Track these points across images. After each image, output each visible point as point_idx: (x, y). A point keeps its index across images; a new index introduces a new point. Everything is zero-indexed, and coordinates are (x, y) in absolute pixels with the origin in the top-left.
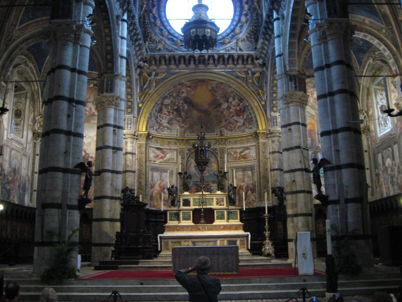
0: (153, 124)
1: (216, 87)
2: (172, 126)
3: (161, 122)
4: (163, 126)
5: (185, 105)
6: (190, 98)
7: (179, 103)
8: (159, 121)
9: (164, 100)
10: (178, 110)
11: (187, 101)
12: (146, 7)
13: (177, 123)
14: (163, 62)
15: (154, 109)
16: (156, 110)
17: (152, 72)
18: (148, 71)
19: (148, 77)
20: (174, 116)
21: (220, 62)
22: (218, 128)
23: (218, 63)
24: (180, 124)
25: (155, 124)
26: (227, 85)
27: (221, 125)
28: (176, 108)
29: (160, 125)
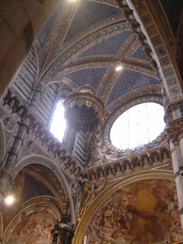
0: (93, 238)
1: (157, 187)
2: (117, 240)
3: (104, 236)
4: (106, 240)
5: (130, 214)
6: (134, 205)
7: (122, 213)
8: (101, 235)
9: (105, 211)
10: (122, 221)
11: (130, 209)
12: (92, 136)
13: (122, 235)
14: (101, 175)
15: (94, 222)
16: (97, 224)
17: (91, 186)
18: (89, 186)
19: (89, 191)
20: (118, 228)
21: (155, 160)
22: (168, 234)
23: (153, 161)
24: (126, 236)
25: (96, 239)
26: (165, 180)
27: (171, 230)
28: (119, 218)
29: (103, 239)
